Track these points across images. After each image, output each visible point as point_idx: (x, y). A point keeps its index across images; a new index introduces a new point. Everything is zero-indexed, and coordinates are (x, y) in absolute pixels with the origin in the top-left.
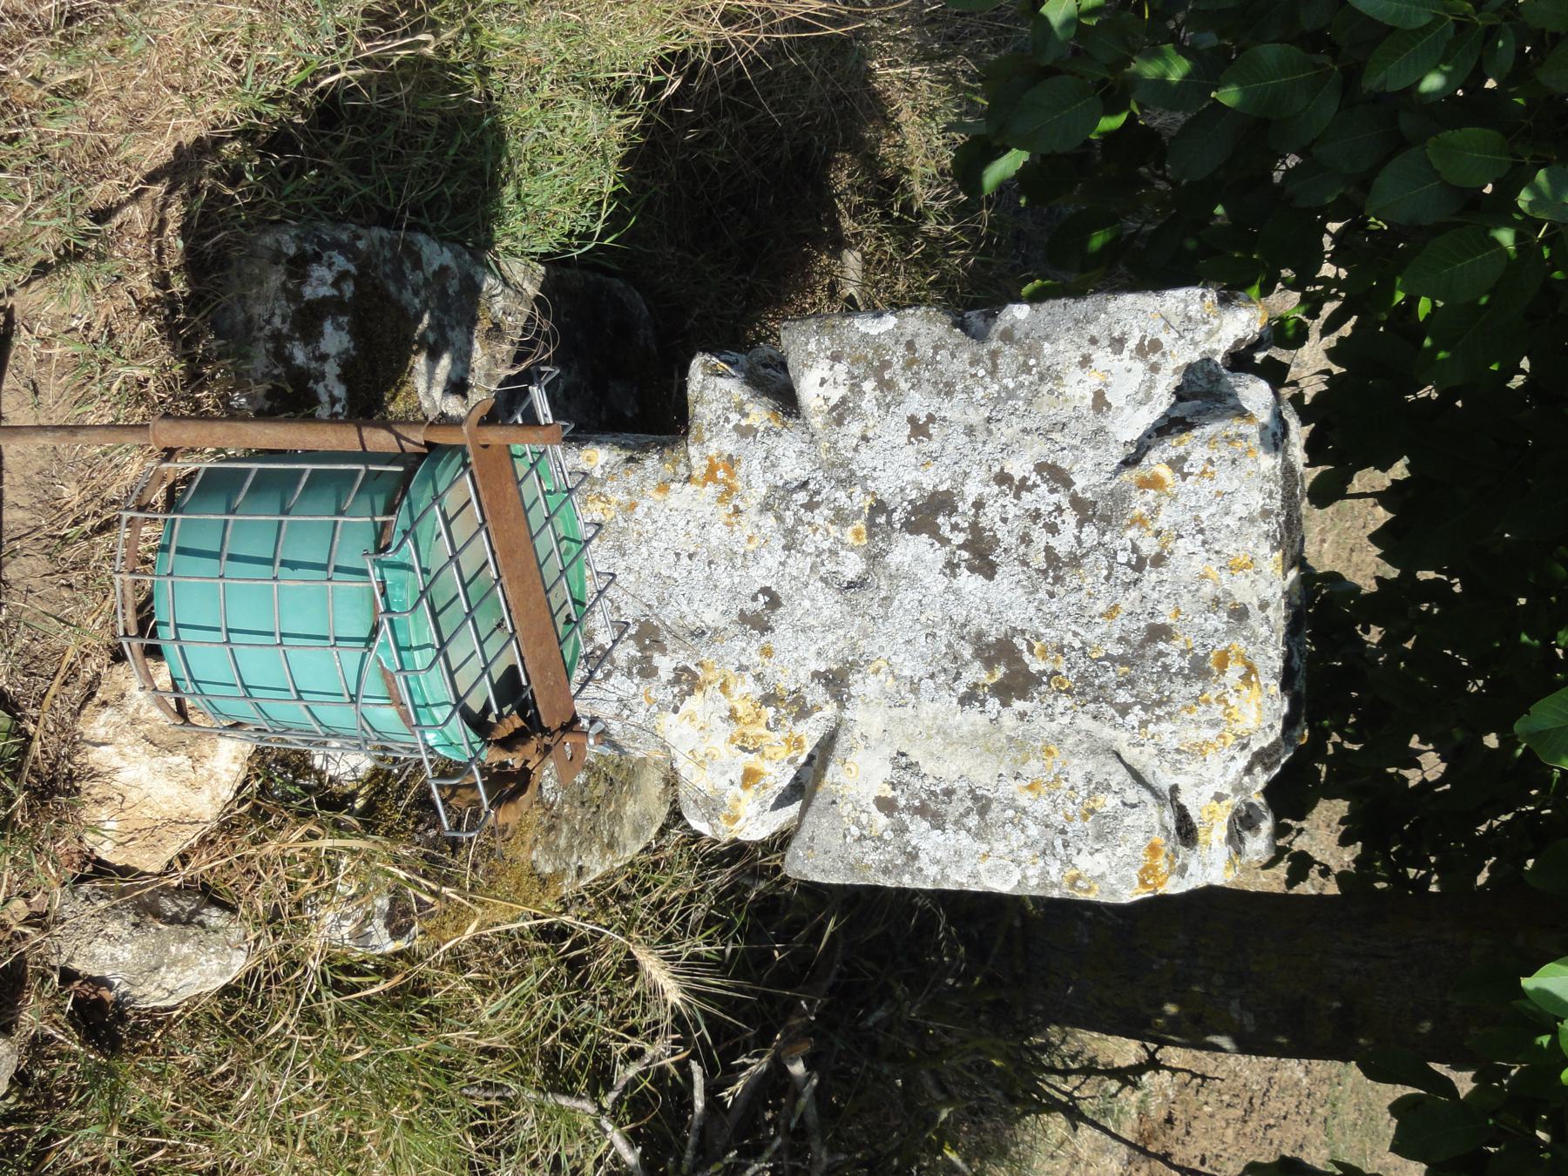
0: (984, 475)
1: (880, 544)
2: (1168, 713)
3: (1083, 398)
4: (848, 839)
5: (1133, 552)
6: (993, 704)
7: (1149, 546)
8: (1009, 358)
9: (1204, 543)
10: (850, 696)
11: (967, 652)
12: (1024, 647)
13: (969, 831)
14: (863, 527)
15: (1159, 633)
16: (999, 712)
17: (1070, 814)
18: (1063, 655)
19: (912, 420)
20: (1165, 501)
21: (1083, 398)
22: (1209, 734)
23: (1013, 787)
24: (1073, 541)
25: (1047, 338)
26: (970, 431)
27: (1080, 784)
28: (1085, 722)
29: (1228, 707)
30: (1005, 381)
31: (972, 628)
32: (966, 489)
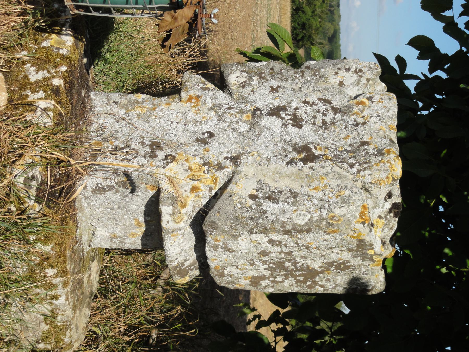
0: (298, 101)
1: (257, 120)
2: (369, 166)
3: (335, 83)
4: (236, 208)
5: (354, 121)
6: (300, 164)
7: (360, 120)
8: (308, 73)
9: (380, 120)
10: (241, 163)
11: (290, 149)
12: (313, 147)
13: (289, 204)
14: (250, 115)
15: (364, 143)
16: (302, 167)
17: (331, 196)
18: (328, 150)
19: (272, 87)
20: (366, 108)
21: (335, 83)
22: (383, 175)
23: (307, 189)
24: (332, 118)
25: (322, 68)
26: (293, 90)
27: (335, 187)
28: (336, 169)
29: (391, 164)
30: (307, 78)
31: (293, 142)
32: (292, 105)
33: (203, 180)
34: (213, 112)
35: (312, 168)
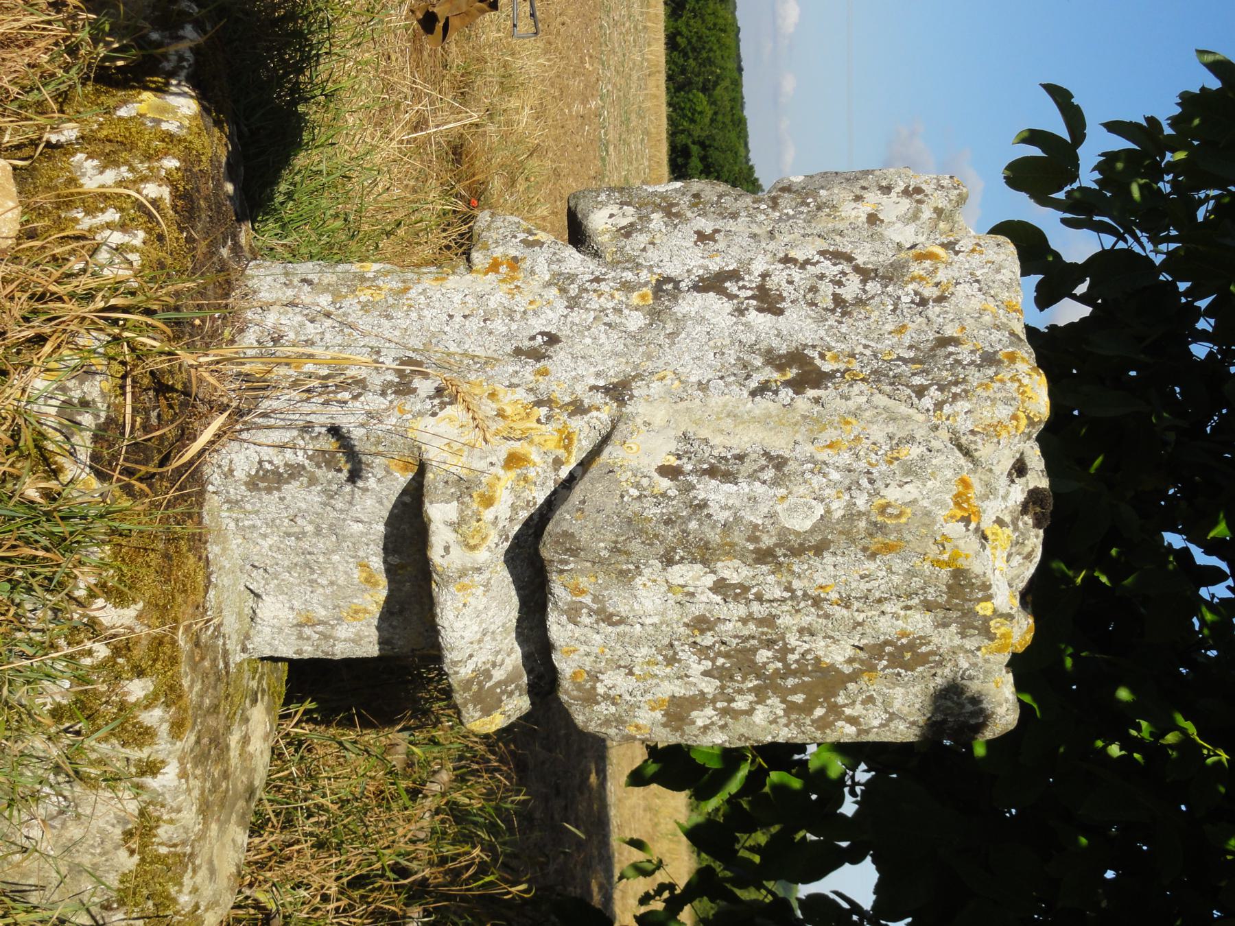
4: (625, 499)
6: (786, 394)
7: (929, 292)
9: (980, 290)
10: (632, 397)
11: (758, 361)
12: (816, 355)
13: (764, 482)
14: (650, 293)
15: (944, 342)
16: (792, 399)
20: (941, 266)
22: (1003, 412)
23: (809, 449)
25: (822, 188)
26: (754, 236)
29: (1021, 385)
31: (763, 346)
32: (753, 267)
33: (536, 439)
34: (554, 291)
35: (817, 400)
